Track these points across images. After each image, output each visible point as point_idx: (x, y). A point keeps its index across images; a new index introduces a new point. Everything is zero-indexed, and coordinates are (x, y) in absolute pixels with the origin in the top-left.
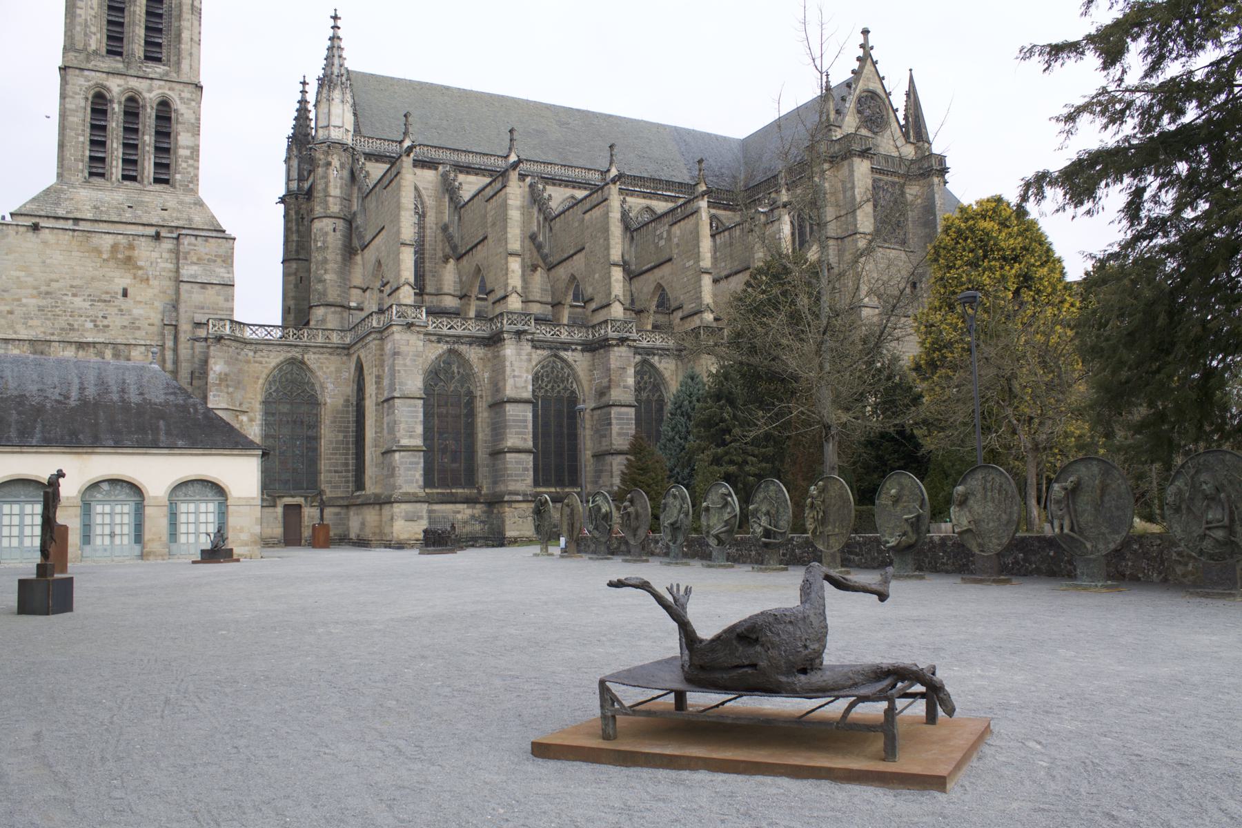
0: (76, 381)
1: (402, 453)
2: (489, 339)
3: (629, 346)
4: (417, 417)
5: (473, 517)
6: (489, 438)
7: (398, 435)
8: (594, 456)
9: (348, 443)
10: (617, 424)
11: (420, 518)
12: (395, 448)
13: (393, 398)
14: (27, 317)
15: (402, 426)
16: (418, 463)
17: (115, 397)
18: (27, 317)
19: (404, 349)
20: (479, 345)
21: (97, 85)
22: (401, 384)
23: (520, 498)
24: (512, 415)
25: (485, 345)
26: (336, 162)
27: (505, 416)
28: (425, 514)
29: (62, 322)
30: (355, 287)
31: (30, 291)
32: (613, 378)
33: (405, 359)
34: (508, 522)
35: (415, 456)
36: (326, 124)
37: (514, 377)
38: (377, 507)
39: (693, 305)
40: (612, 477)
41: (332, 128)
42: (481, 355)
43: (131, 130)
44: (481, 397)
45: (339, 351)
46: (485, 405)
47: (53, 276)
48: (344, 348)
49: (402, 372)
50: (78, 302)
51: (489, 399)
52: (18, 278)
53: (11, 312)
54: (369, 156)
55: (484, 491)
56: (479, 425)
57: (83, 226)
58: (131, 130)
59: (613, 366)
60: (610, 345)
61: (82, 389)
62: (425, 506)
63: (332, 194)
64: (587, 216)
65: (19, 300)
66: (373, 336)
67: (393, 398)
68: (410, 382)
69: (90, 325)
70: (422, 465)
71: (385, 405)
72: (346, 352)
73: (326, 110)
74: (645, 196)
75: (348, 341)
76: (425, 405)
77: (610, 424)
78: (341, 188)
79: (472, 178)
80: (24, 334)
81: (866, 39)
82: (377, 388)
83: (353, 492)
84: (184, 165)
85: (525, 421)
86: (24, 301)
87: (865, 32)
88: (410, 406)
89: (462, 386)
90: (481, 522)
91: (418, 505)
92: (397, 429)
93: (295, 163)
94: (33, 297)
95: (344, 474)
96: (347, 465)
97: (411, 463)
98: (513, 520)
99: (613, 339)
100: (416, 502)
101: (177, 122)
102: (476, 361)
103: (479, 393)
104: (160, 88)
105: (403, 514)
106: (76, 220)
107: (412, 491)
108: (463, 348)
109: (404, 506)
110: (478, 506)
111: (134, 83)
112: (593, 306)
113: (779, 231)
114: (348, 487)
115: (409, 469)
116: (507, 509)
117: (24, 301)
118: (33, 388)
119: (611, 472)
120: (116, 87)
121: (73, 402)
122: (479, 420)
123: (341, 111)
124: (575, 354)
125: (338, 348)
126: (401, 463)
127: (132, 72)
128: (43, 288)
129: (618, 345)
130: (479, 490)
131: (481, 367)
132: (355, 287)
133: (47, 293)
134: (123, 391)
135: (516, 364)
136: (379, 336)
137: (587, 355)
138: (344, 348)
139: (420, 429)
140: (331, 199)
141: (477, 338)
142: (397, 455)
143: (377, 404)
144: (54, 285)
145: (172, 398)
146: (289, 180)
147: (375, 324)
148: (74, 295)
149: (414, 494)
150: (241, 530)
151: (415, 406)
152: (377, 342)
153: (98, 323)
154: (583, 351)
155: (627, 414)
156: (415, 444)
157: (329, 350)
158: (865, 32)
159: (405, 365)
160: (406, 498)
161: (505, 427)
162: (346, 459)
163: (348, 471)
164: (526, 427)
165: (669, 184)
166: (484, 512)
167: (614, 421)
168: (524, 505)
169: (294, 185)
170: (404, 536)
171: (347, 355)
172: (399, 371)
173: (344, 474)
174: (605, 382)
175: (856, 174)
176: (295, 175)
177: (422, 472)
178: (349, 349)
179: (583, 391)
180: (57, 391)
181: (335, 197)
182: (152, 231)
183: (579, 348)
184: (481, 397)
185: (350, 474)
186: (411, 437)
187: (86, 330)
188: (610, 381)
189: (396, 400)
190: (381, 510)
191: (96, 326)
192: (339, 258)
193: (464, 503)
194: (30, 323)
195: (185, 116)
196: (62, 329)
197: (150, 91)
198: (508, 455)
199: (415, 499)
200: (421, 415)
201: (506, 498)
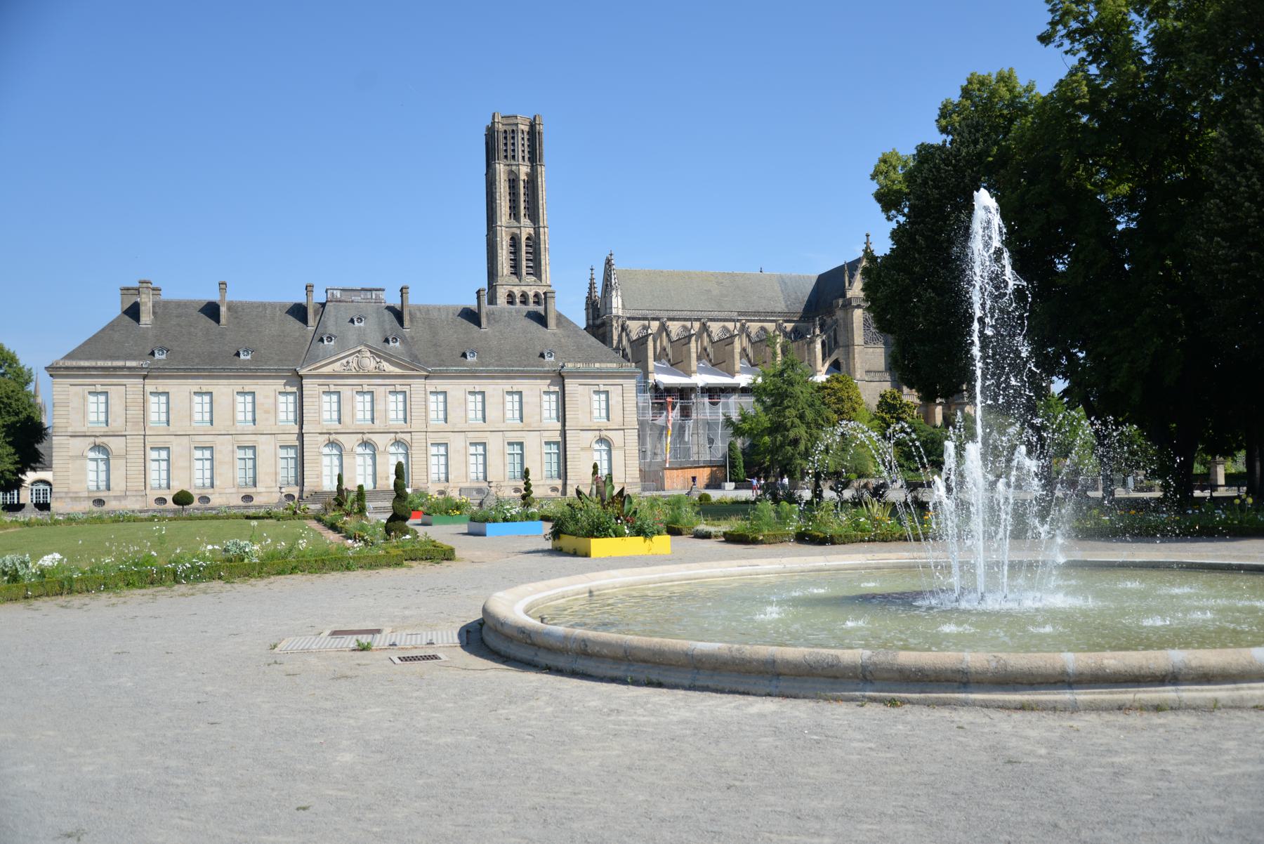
54: (629, 319)
64: (727, 347)
74: (760, 321)
79: (675, 323)
81: (868, 239)
87: (868, 236)
93: (591, 311)
111: (524, 288)
113: (815, 348)
127: (522, 283)
146: (588, 319)
158: (868, 236)
165: (772, 313)
169: (591, 322)
175: (854, 317)
176: (591, 317)
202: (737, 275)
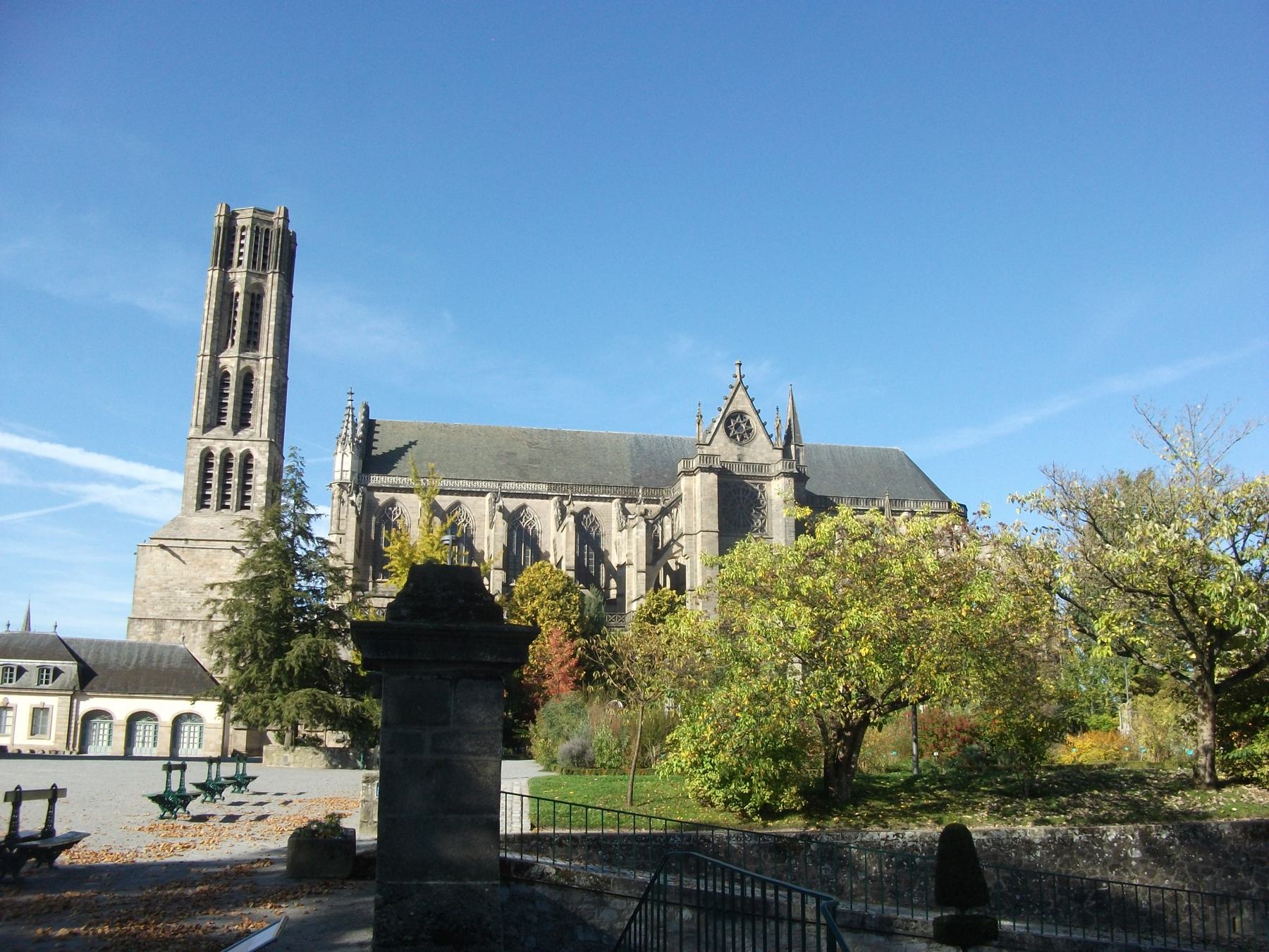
0: (136, 656)
14: (154, 604)
17: (154, 664)
18: (154, 604)
21: (208, 448)
29: (173, 607)
31: (157, 588)
43: (225, 476)
47: (169, 577)
50: (183, 592)
52: (150, 579)
53: (144, 601)
57: (191, 544)
58: (225, 476)
61: (139, 659)
65: (149, 593)
69: (189, 608)
80: (151, 614)
84: (259, 496)
86: (152, 594)
94: (158, 591)
101: (257, 468)
104: (247, 445)
106: (186, 540)
111: (230, 444)
117: (152, 594)
118: (113, 659)
120: (218, 449)
121: (130, 667)
128: (164, 585)
133: (166, 588)
134: (160, 661)
144: (170, 583)
145: (186, 665)
148: (182, 589)
150: (211, 742)
153: (195, 607)
180: (125, 661)
182: (230, 544)
187: (188, 612)
191: (194, 609)
194: (156, 608)
195: (262, 463)
196: (173, 611)
197: (240, 448)
202: (565, 432)
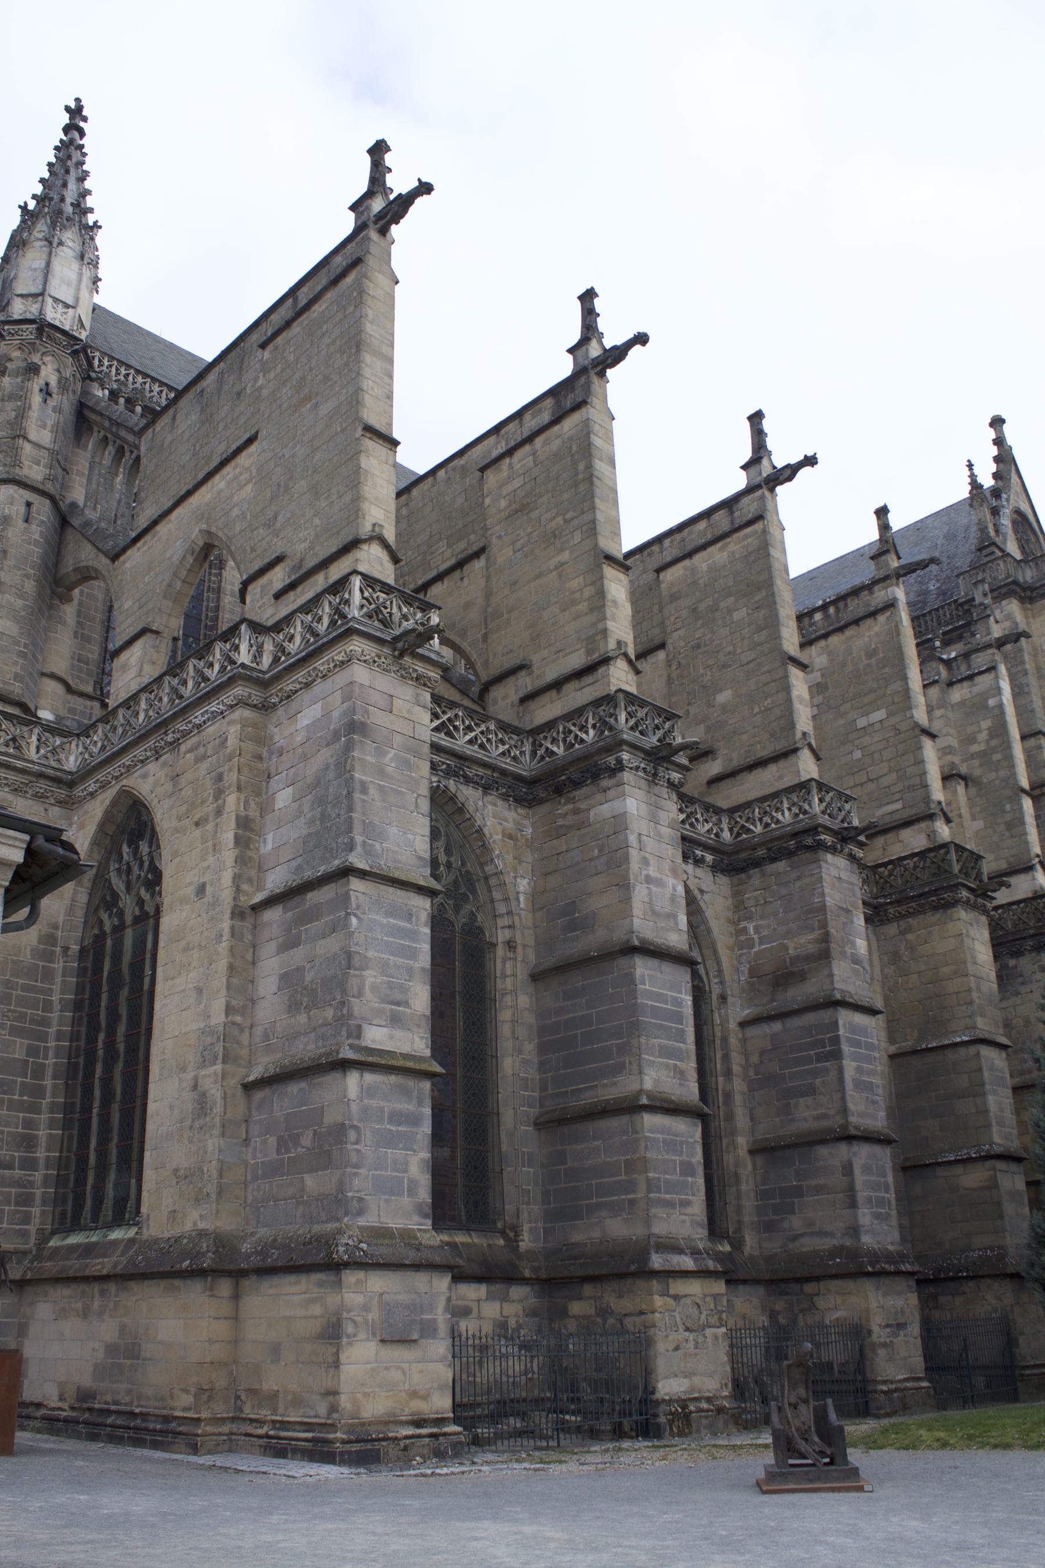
1: (369, 1078)
2: (532, 782)
3: (852, 857)
4: (413, 954)
5: (502, 1325)
6: (532, 1074)
7: (358, 1007)
8: (752, 1152)
9: (39, 1072)
10: (855, 1057)
11: (428, 1330)
12: (347, 1054)
13: (347, 872)
15: (371, 977)
16: (414, 1120)
19: (378, 718)
20: (505, 797)
22: (369, 828)
23: (687, 1263)
24: (650, 995)
25: (519, 801)
26: (49, 373)
27: (633, 993)
28: (441, 1317)
30: (53, 676)
32: (833, 931)
33: (380, 752)
34: (662, 1345)
35: (406, 1093)
36: (33, 290)
37: (648, 879)
38: (225, 1287)
39: (898, 805)
40: (853, 1204)
41: (49, 301)
42: (510, 825)
44: (510, 945)
45: (42, 785)
46: (522, 973)
48: (57, 781)
49: (372, 791)
51: (532, 957)
55: (526, 1243)
56: (505, 1030)
59: (829, 901)
60: (820, 845)
62: (442, 1283)
63: (33, 436)
66: (239, 691)
67: (347, 872)
68: (393, 831)
70: (426, 1128)
71: (273, 915)
72: (62, 793)
73: (40, 264)
75: (71, 762)
76: (438, 922)
77: (836, 1055)
78: (55, 430)
82: (241, 860)
83: (44, 1238)
85: (679, 1017)
88: (393, 911)
89: (457, 909)
90: (524, 1346)
91: (421, 1281)
92: (353, 983)
95: (18, 1173)
96: (28, 1142)
97: (397, 1118)
98: (673, 1336)
99: (828, 830)
100: (417, 1267)
102: (498, 837)
103: (502, 936)
105: (374, 1315)
107: (396, 1223)
108: (469, 795)
109: (378, 1283)
110: (517, 1292)
112: (714, 767)
114: (27, 1219)
115: (388, 1140)
116: (658, 1301)
119: (850, 1193)
122: (505, 1015)
123: (73, 277)
124: (699, 872)
125: (41, 775)
126: (365, 1111)
129: (833, 850)
130: (512, 1244)
131: (510, 858)
132: (53, 676)
135: (650, 844)
136: (256, 695)
137: (723, 880)
138: (57, 781)
139: (420, 998)
140: (28, 448)
141: (504, 773)
142: (353, 1082)
143: (238, 913)
147: (244, 656)
149: (406, 1235)
151: (409, 916)
152: (247, 713)
154: (715, 868)
155: (863, 1031)
156: (405, 1049)
157: (12, 776)
159: (381, 772)
160: (383, 1251)
161: (635, 1028)
162: (29, 1124)
163: (29, 1164)
164: (680, 1036)
166: (533, 1313)
167: (846, 1048)
168: (694, 1288)
170: (374, 1408)
171: (61, 803)
172: (364, 790)
173: (18, 1173)
174: (803, 943)
177: (426, 1155)
178: (71, 785)
179: (720, 971)
181: (37, 445)
183: (709, 858)
184: (510, 945)
185: (38, 1176)
186: (395, 1021)
188: (826, 938)
189: (356, 884)
190: (236, 1297)
192: (30, 586)
193: (479, 1279)
198: (649, 1120)
199: (411, 1256)
200: (426, 947)
201: (657, 1261)
